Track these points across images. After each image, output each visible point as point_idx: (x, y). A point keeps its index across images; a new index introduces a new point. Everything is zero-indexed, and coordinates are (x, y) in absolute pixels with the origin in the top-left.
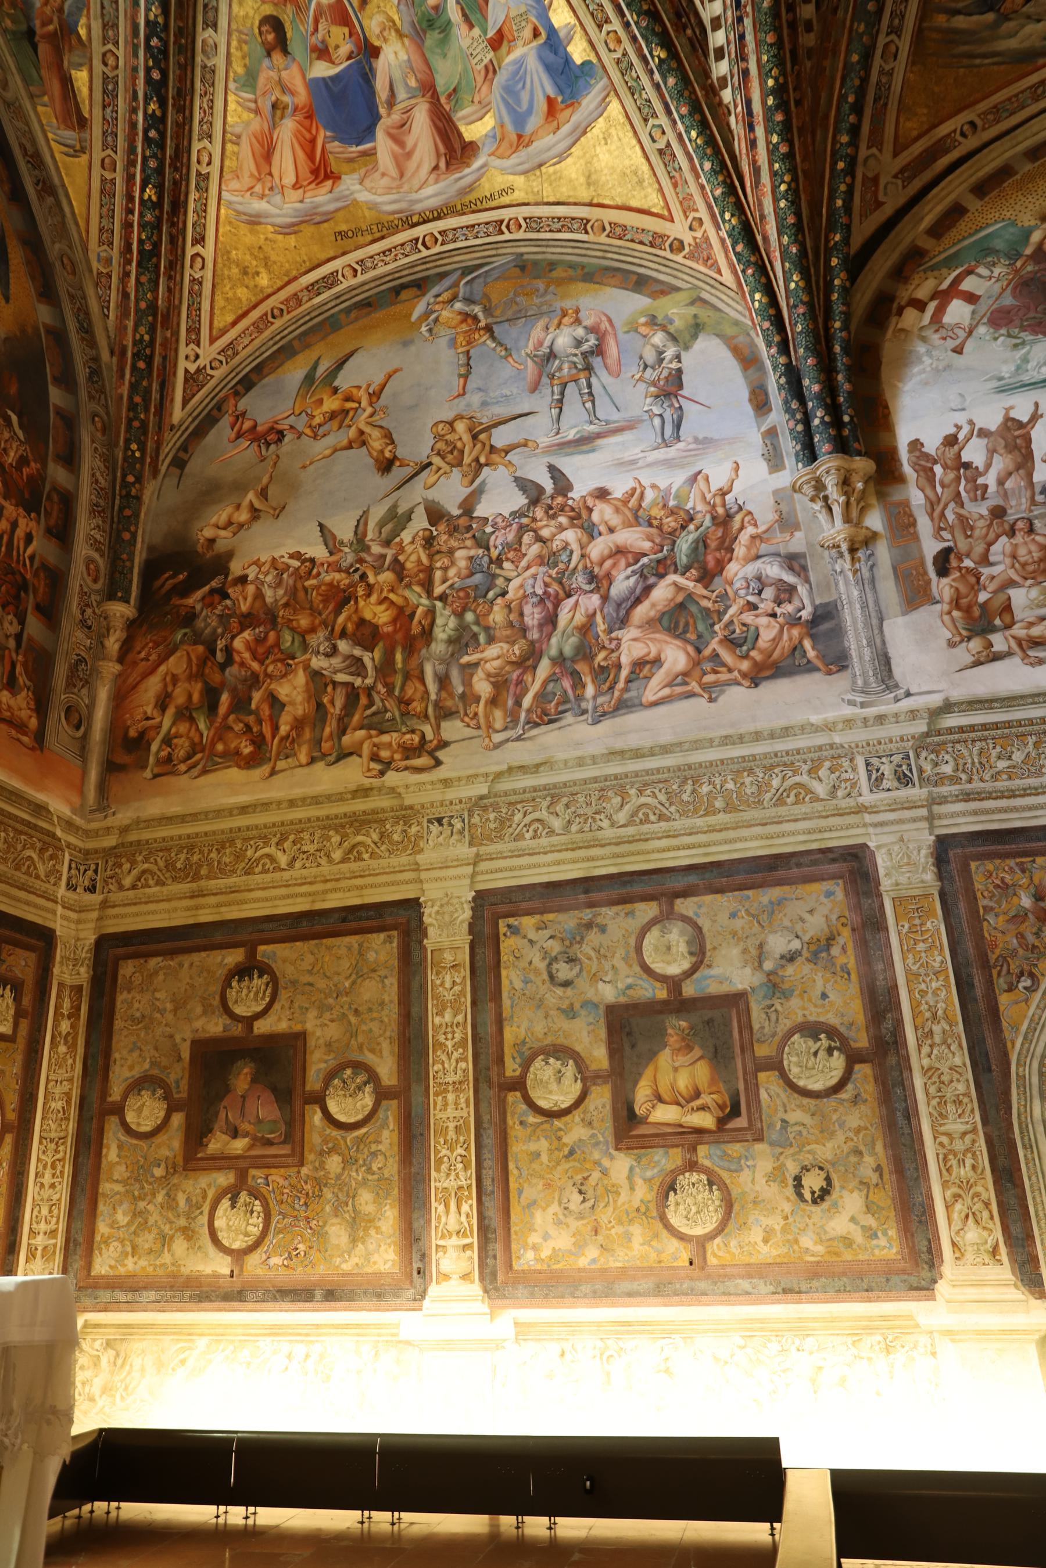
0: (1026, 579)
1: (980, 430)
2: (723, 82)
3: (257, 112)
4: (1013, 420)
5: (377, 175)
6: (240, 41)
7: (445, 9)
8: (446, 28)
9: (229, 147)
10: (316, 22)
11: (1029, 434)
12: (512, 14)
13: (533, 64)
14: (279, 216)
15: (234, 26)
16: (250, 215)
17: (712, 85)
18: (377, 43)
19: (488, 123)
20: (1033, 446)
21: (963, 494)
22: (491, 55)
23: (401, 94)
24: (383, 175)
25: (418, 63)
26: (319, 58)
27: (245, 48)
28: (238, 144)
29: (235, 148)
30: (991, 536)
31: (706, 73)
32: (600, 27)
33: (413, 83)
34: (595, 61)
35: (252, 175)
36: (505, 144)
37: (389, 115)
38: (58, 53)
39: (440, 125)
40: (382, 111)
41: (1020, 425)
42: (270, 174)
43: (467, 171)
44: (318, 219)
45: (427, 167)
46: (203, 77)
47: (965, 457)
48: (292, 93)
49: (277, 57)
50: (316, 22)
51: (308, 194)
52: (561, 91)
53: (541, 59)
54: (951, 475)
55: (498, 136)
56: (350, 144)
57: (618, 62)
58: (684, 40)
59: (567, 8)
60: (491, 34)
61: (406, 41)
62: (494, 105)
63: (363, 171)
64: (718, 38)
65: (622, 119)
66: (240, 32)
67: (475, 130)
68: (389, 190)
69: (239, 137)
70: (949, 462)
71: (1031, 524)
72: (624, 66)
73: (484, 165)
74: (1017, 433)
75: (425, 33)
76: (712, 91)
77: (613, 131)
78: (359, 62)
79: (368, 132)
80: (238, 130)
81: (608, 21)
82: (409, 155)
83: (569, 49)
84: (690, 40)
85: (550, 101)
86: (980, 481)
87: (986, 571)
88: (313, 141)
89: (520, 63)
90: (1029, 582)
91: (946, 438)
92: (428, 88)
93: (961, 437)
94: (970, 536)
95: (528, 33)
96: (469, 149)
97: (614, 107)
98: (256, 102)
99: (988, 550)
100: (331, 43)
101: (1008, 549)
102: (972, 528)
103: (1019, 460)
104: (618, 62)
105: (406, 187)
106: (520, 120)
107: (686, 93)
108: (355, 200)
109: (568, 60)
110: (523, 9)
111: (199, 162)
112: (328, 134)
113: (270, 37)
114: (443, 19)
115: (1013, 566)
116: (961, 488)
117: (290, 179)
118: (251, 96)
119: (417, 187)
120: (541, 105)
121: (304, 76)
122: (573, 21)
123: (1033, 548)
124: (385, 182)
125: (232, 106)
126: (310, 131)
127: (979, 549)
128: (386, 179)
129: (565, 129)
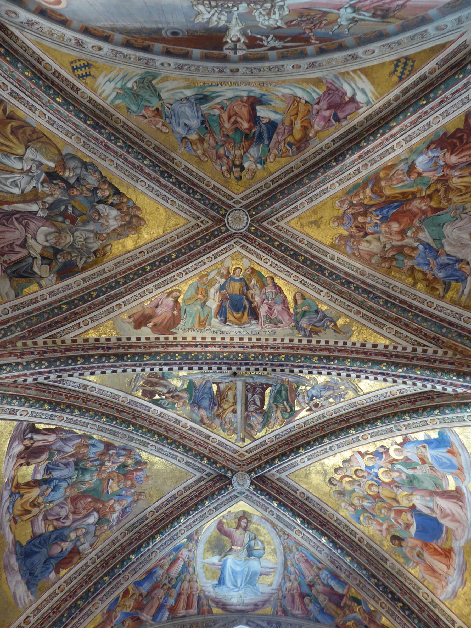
2: (454, 390)
3: (418, 564)
5: (456, 532)
6: (394, 554)
7: (408, 474)
8: (414, 477)
9: (425, 583)
10: (398, 522)
12: (416, 452)
13: (435, 452)
14: (457, 583)
15: (389, 553)
16: (452, 594)
17: (455, 395)
18: (411, 504)
19: (450, 478)
22: (427, 466)
23: (431, 505)
24: (457, 529)
25: (422, 493)
26: (409, 528)
27: (397, 554)
28: (425, 579)
29: (426, 581)
31: (451, 395)
32: (427, 424)
33: (428, 498)
34: (438, 430)
35: (438, 582)
36: (460, 475)
37: (436, 514)
38: (374, 622)
39: (446, 496)
40: (434, 515)
42: (441, 575)
43: (466, 495)
44: (464, 567)
45: (460, 510)
46: (400, 575)
48: (416, 546)
49: (404, 544)
50: (398, 522)
51: (453, 565)
52: (446, 446)
53: (433, 449)
55: (457, 477)
56: (441, 535)
57: (441, 422)
58: (437, 400)
59: (419, 433)
60: (420, 463)
61: (414, 493)
62: (445, 473)
63: (453, 537)
64: (439, 388)
65: (462, 429)
66: (392, 552)
67: (452, 485)
68: (463, 531)
69: (423, 577)
72: (443, 421)
73: (466, 487)
75: (413, 485)
76: (457, 395)
77: (465, 434)
78: (415, 514)
79: (440, 525)
80: (421, 576)
81: (426, 421)
82: (453, 515)
83: (432, 438)
84: (438, 397)
85: (449, 452)
88: (435, 549)
89: (432, 457)
92: (432, 494)
95: (423, 450)
96: (458, 490)
97: (457, 430)
98: (414, 562)
100: (406, 521)
104: (441, 422)
105: (465, 523)
106: (452, 466)
107: (453, 408)
108: (462, 547)
109: (436, 440)
110: (415, 448)
111: (426, 599)
112: (435, 541)
113: (397, 542)
114: (411, 476)
117: (445, 568)
118: (412, 563)
119: (466, 519)
120: (449, 456)
121: (412, 538)
122: (423, 433)
124: (460, 530)
125: (413, 572)
126: (431, 548)
128: (459, 529)
129: (460, 451)
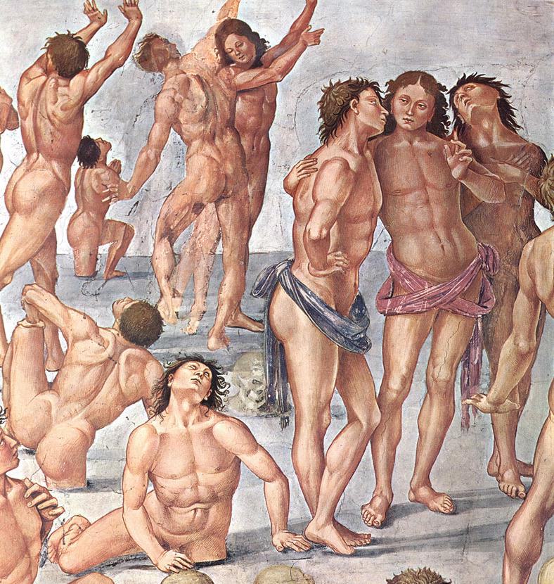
0: (166, 546)
1: (151, 39)
4: (242, 29)
11: (271, 86)
20: (274, 133)
21: (63, 246)
30: (107, 394)
41: (259, 55)
47: (91, 129)
54: (42, 177)
70: (46, 128)
71: (216, 383)
74: (242, 78)
86: (116, 212)
87: (73, 505)
90: (171, 557)
91: (57, 43)
93: (95, 49)
94: (51, 386)
99: (88, 440)
101: (141, 445)
102: (62, 361)
103: (229, 168)
115: (141, 503)
116: (61, 227)
123: (205, 457)
127: (64, 434)
